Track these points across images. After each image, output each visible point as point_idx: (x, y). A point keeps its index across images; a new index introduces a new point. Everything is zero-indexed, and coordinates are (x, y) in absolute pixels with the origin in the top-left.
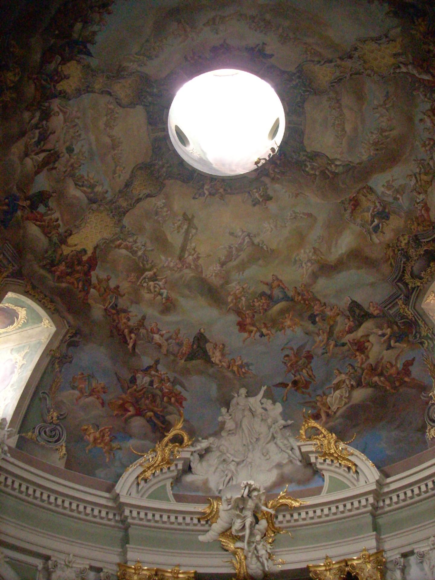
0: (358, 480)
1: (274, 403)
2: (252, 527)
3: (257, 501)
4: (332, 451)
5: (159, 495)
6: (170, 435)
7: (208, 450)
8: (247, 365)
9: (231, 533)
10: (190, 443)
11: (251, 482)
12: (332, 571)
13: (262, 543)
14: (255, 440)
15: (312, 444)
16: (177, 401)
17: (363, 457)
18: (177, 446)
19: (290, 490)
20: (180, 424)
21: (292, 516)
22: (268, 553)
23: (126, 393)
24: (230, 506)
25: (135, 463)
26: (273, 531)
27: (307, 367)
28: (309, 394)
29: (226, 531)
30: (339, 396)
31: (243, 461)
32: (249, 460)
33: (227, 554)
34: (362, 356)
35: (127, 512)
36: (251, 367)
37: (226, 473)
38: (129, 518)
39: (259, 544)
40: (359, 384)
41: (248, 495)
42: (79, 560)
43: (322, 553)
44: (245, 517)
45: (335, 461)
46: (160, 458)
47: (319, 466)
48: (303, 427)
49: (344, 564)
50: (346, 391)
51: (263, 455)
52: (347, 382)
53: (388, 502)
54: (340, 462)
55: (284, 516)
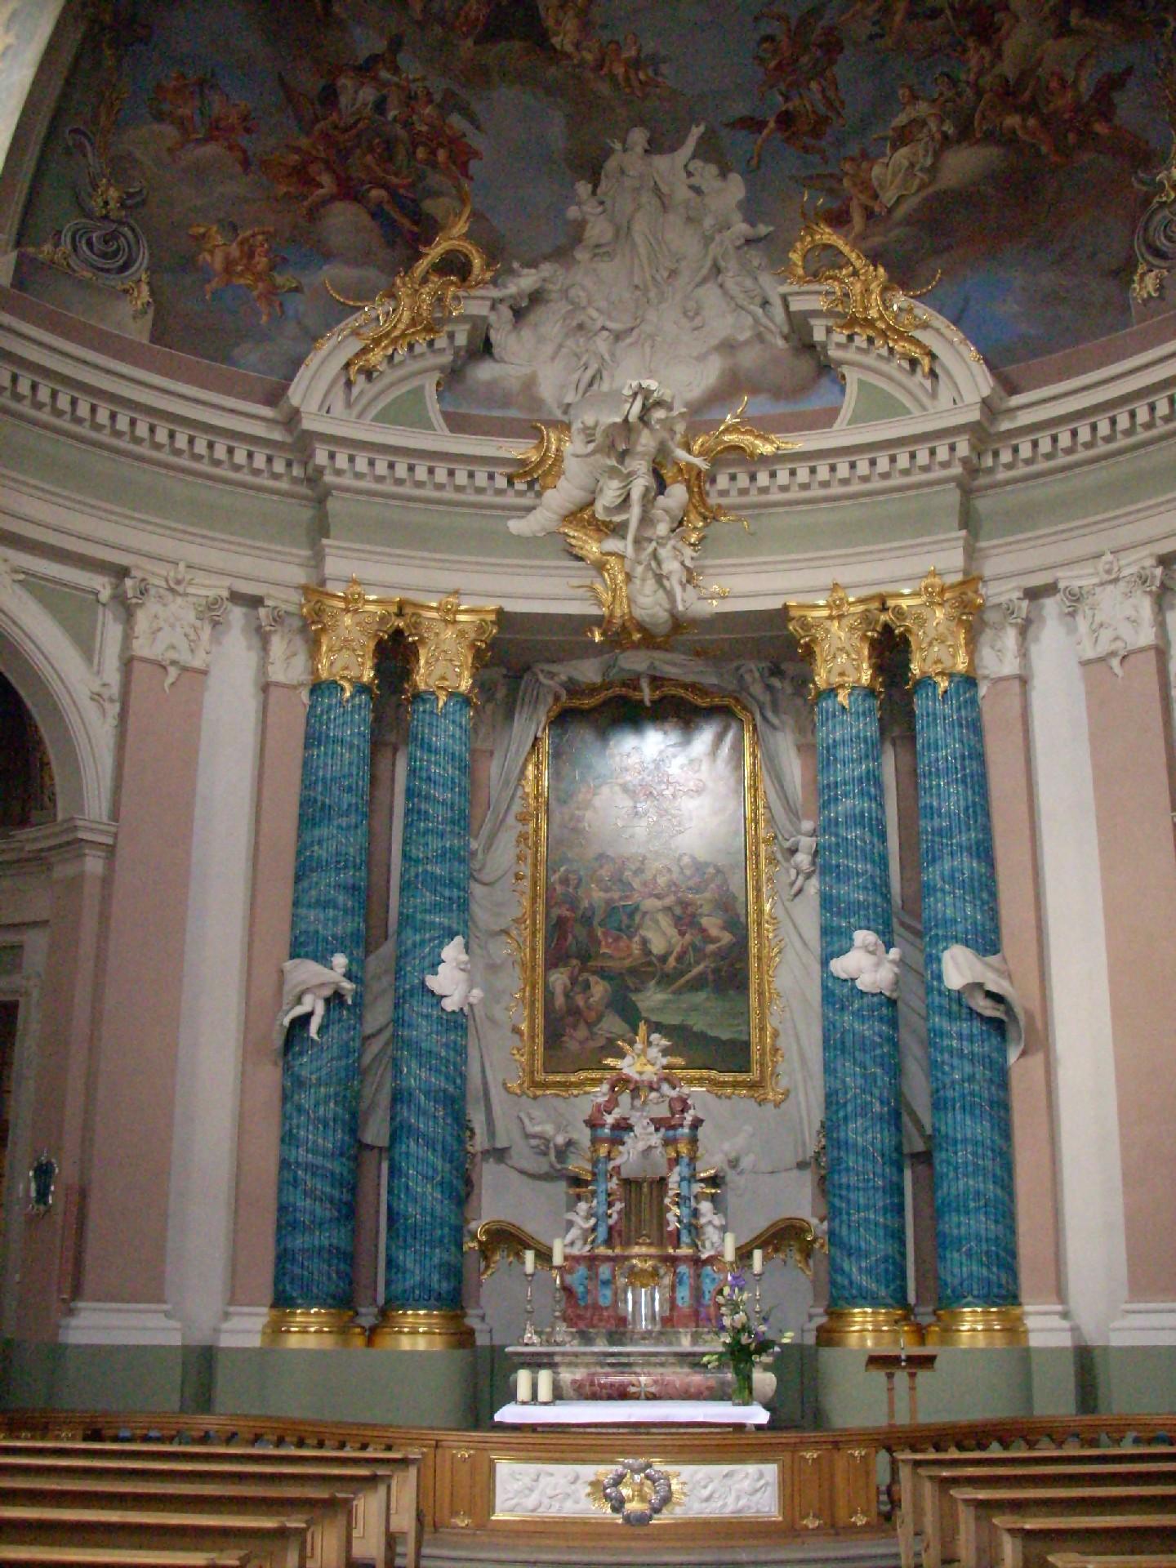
0: (934, 395)
1: (723, 174)
2: (648, 501)
3: (665, 435)
4: (873, 313)
5: (406, 412)
6: (434, 253)
7: (536, 298)
8: (655, 61)
9: (593, 516)
10: (488, 275)
11: (652, 384)
12: (845, 621)
13: (672, 542)
14: (666, 274)
15: (819, 293)
16: (452, 157)
17: (956, 336)
18: (452, 283)
19: (752, 412)
20: (461, 223)
21: (753, 478)
22: (688, 570)
23: (308, 134)
24: (591, 446)
25: (342, 326)
26: (701, 514)
27: (821, 74)
28: (822, 152)
29: (582, 509)
30: (906, 163)
31: (632, 329)
32: (647, 328)
33: (580, 568)
34: (983, 50)
35: (321, 457)
36: (665, 69)
37: (584, 359)
38: (327, 471)
39: (663, 545)
40: (965, 133)
41: (641, 418)
42: (201, 578)
43: (825, 577)
44: (630, 474)
45: (879, 342)
46: (406, 316)
47: (833, 353)
48: (798, 245)
49: (876, 605)
50: (927, 151)
51: (685, 313)
52: (933, 125)
53: (1006, 457)
55: (733, 478)
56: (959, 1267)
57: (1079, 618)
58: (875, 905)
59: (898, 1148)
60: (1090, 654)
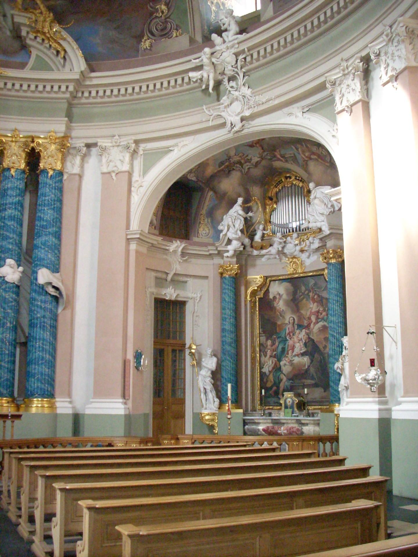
0: (64, 66)
4: (46, 30)
12: (17, 144)
15: (27, 17)
17: (75, 46)
45: (46, 41)
47: (28, 42)
49: (30, 139)
53: (86, 94)
54: (51, 43)
56: (34, 384)
57: (103, 157)
58: (15, 250)
59: (15, 340)
60: (105, 170)
